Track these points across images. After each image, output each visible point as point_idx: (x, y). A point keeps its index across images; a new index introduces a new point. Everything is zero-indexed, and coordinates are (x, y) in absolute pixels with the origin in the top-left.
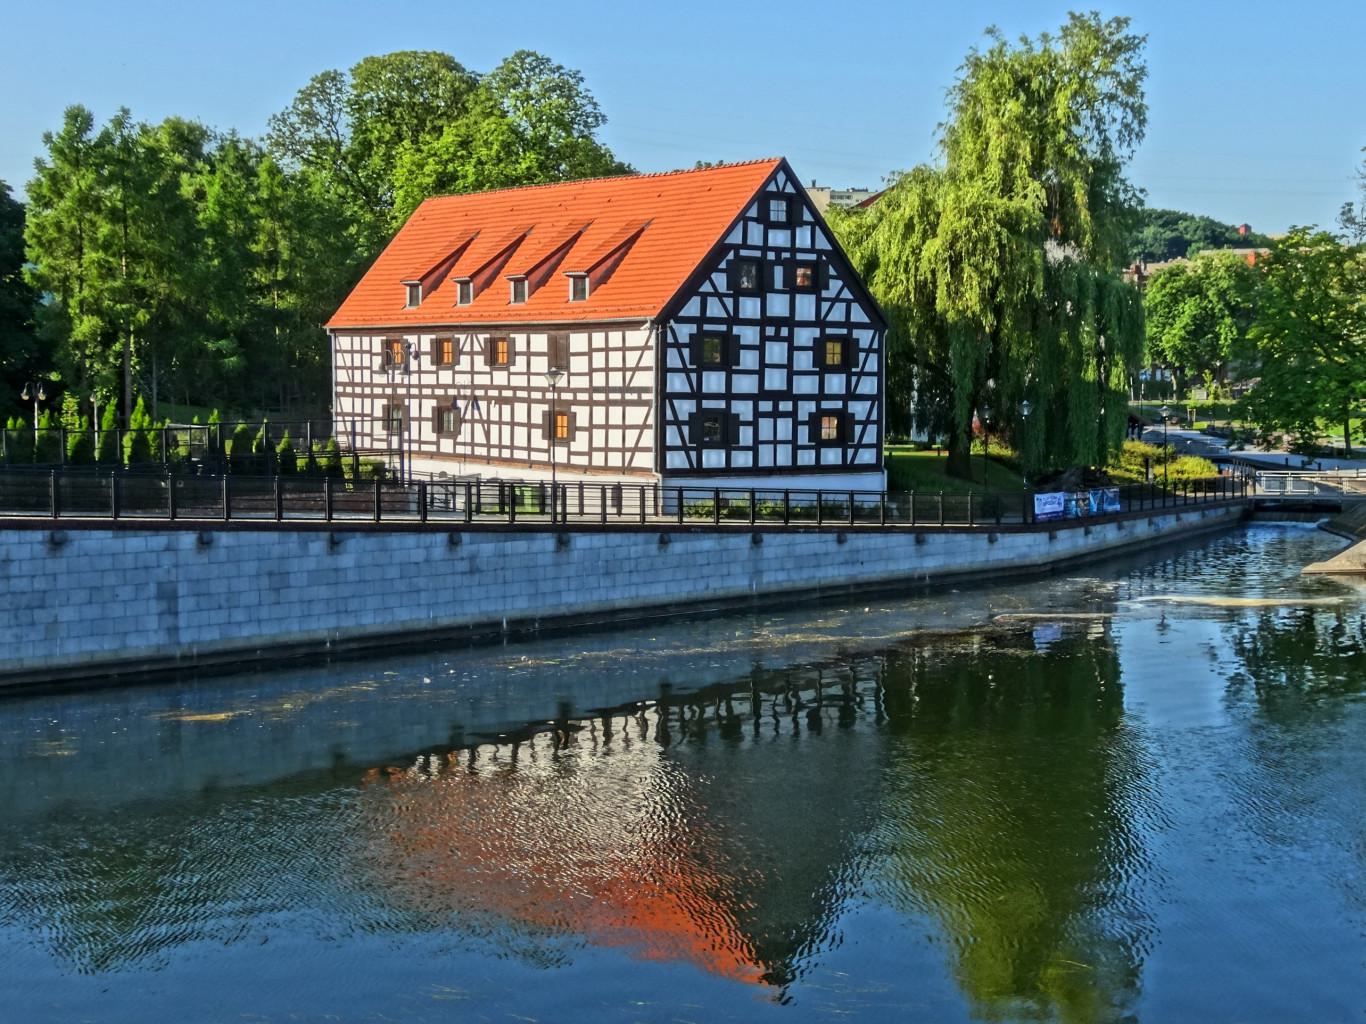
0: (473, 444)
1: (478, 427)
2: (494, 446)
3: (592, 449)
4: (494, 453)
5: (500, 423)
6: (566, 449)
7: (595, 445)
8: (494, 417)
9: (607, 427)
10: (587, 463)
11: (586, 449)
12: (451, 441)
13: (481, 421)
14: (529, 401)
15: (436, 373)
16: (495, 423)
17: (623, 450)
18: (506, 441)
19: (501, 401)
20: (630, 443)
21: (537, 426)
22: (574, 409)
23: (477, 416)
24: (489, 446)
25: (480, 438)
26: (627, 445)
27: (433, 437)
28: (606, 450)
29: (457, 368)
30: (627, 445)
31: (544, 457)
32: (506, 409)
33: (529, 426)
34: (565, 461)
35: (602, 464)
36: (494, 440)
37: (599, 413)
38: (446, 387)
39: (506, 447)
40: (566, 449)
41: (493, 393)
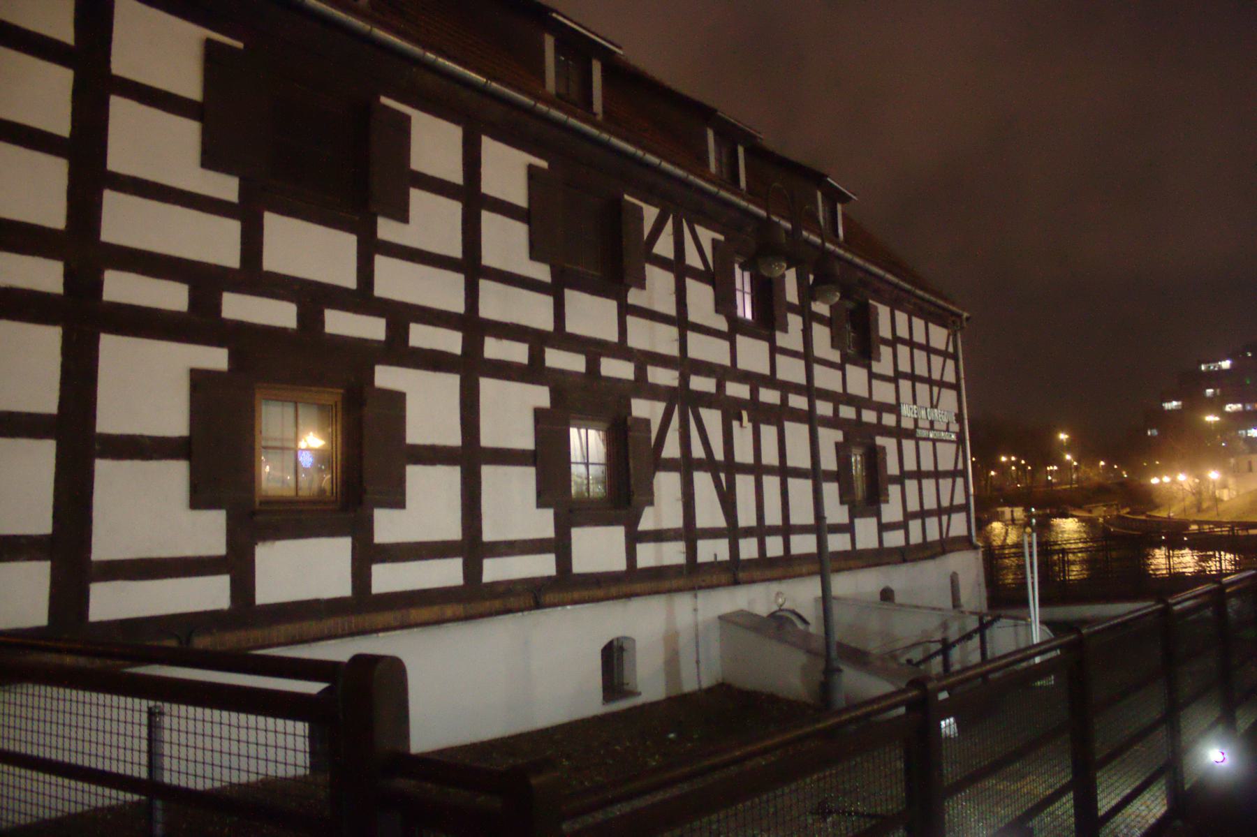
0: (690, 534)
1: (703, 481)
2: (748, 532)
3: (908, 516)
4: (748, 549)
5: (757, 470)
6: (874, 521)
8: (744, 454)
12: (617, 534)
13: (709, 464)
14: (809, 418)
15: (555, 290)
16: (745, 469)
18: (773, 517)
19: (762, 414)
23: (698, 451)
24: (733, 532)
25: (709, 513)
27: (543, 524)
29: (634, 297)
32: (769, 433)
33: (815, 474)
36: (746, 517)
38: (593, 349)
39: (773, 531)
40: (874, 521)
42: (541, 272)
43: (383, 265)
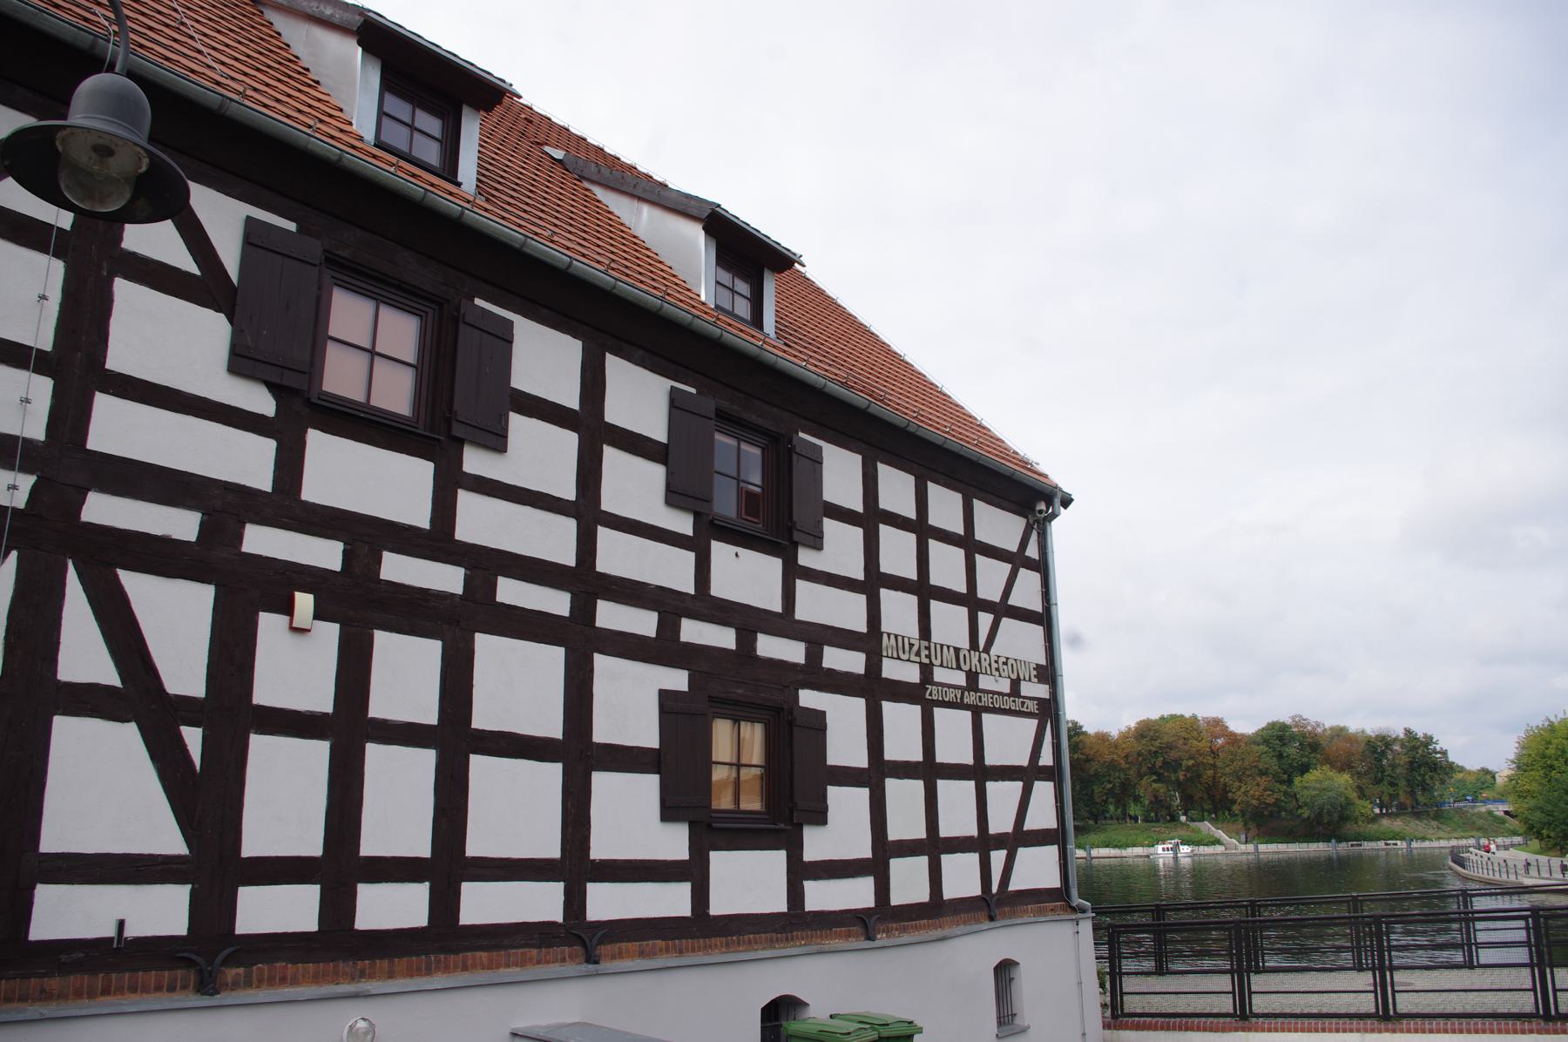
3: (885, 850)
6: (778, 858)
7: (895, 833)
9: (929, 771)
10: (869, 902)
11: (861, 847)
17: (983, 843)
20: (1001, 822)
21: (625, 759)
22: (809, 698)
26: (994, 829)
28: (934, 846)
30: (994, 829)
31: (673, 900)
34: (781, 906)
35: (923, 895)
37: (901, 722)
40: (778, 858)
41: (326, 554)
42: (683, 524)
43: (468, 504)
